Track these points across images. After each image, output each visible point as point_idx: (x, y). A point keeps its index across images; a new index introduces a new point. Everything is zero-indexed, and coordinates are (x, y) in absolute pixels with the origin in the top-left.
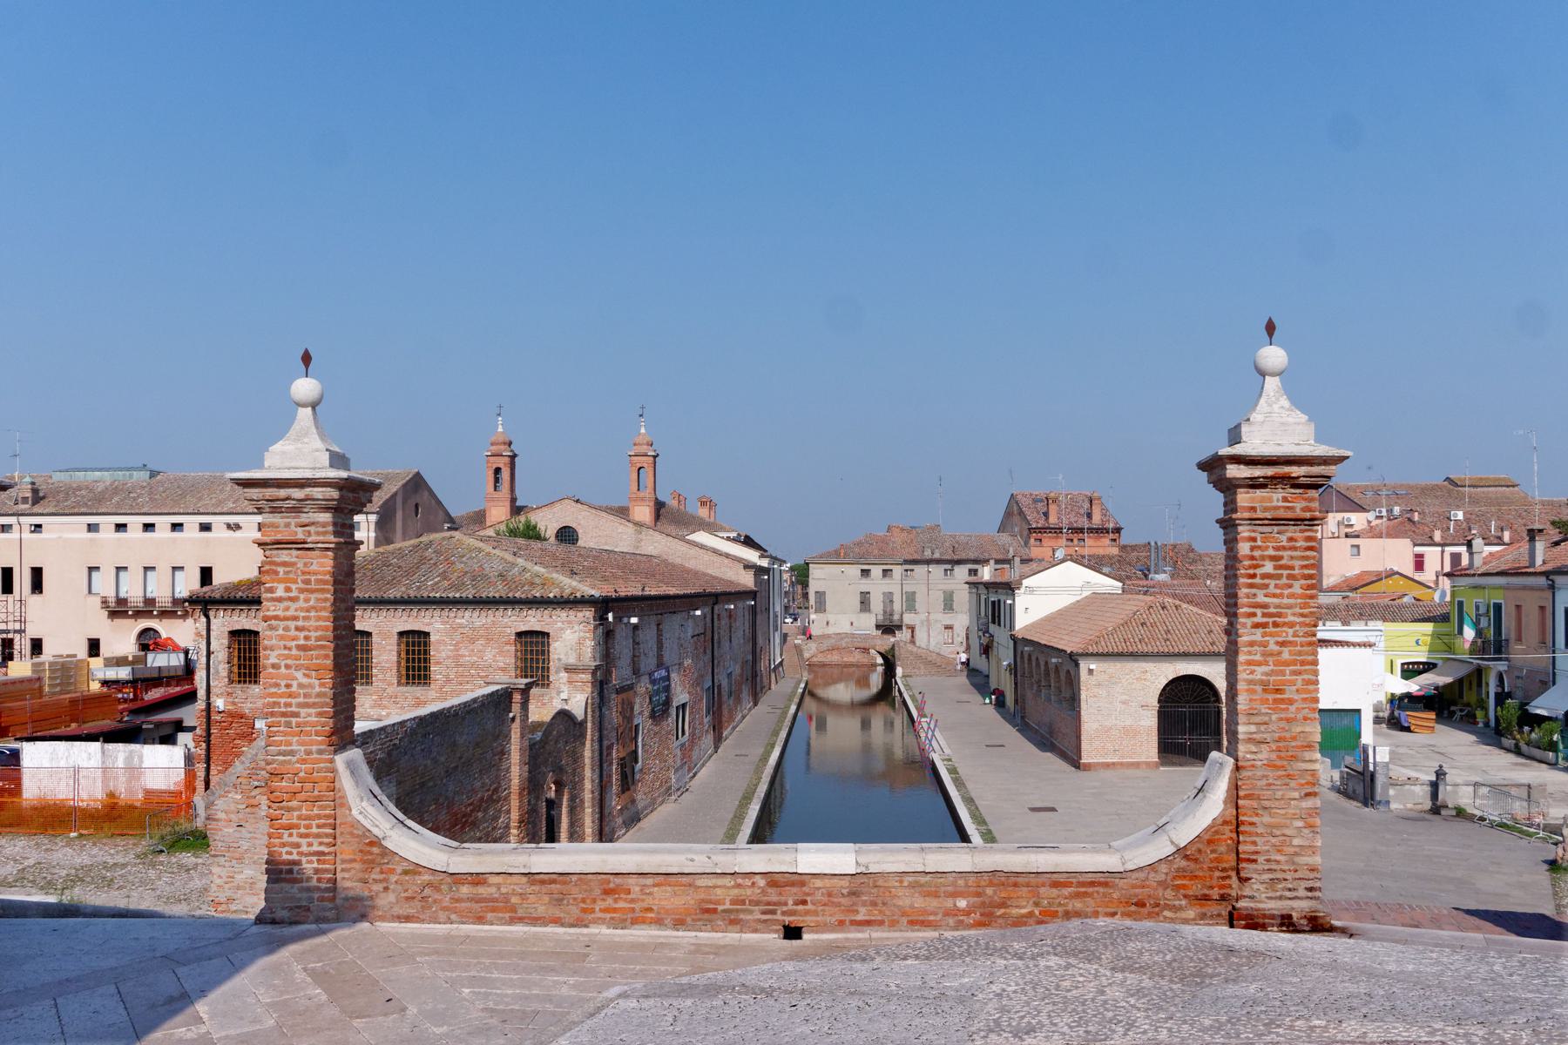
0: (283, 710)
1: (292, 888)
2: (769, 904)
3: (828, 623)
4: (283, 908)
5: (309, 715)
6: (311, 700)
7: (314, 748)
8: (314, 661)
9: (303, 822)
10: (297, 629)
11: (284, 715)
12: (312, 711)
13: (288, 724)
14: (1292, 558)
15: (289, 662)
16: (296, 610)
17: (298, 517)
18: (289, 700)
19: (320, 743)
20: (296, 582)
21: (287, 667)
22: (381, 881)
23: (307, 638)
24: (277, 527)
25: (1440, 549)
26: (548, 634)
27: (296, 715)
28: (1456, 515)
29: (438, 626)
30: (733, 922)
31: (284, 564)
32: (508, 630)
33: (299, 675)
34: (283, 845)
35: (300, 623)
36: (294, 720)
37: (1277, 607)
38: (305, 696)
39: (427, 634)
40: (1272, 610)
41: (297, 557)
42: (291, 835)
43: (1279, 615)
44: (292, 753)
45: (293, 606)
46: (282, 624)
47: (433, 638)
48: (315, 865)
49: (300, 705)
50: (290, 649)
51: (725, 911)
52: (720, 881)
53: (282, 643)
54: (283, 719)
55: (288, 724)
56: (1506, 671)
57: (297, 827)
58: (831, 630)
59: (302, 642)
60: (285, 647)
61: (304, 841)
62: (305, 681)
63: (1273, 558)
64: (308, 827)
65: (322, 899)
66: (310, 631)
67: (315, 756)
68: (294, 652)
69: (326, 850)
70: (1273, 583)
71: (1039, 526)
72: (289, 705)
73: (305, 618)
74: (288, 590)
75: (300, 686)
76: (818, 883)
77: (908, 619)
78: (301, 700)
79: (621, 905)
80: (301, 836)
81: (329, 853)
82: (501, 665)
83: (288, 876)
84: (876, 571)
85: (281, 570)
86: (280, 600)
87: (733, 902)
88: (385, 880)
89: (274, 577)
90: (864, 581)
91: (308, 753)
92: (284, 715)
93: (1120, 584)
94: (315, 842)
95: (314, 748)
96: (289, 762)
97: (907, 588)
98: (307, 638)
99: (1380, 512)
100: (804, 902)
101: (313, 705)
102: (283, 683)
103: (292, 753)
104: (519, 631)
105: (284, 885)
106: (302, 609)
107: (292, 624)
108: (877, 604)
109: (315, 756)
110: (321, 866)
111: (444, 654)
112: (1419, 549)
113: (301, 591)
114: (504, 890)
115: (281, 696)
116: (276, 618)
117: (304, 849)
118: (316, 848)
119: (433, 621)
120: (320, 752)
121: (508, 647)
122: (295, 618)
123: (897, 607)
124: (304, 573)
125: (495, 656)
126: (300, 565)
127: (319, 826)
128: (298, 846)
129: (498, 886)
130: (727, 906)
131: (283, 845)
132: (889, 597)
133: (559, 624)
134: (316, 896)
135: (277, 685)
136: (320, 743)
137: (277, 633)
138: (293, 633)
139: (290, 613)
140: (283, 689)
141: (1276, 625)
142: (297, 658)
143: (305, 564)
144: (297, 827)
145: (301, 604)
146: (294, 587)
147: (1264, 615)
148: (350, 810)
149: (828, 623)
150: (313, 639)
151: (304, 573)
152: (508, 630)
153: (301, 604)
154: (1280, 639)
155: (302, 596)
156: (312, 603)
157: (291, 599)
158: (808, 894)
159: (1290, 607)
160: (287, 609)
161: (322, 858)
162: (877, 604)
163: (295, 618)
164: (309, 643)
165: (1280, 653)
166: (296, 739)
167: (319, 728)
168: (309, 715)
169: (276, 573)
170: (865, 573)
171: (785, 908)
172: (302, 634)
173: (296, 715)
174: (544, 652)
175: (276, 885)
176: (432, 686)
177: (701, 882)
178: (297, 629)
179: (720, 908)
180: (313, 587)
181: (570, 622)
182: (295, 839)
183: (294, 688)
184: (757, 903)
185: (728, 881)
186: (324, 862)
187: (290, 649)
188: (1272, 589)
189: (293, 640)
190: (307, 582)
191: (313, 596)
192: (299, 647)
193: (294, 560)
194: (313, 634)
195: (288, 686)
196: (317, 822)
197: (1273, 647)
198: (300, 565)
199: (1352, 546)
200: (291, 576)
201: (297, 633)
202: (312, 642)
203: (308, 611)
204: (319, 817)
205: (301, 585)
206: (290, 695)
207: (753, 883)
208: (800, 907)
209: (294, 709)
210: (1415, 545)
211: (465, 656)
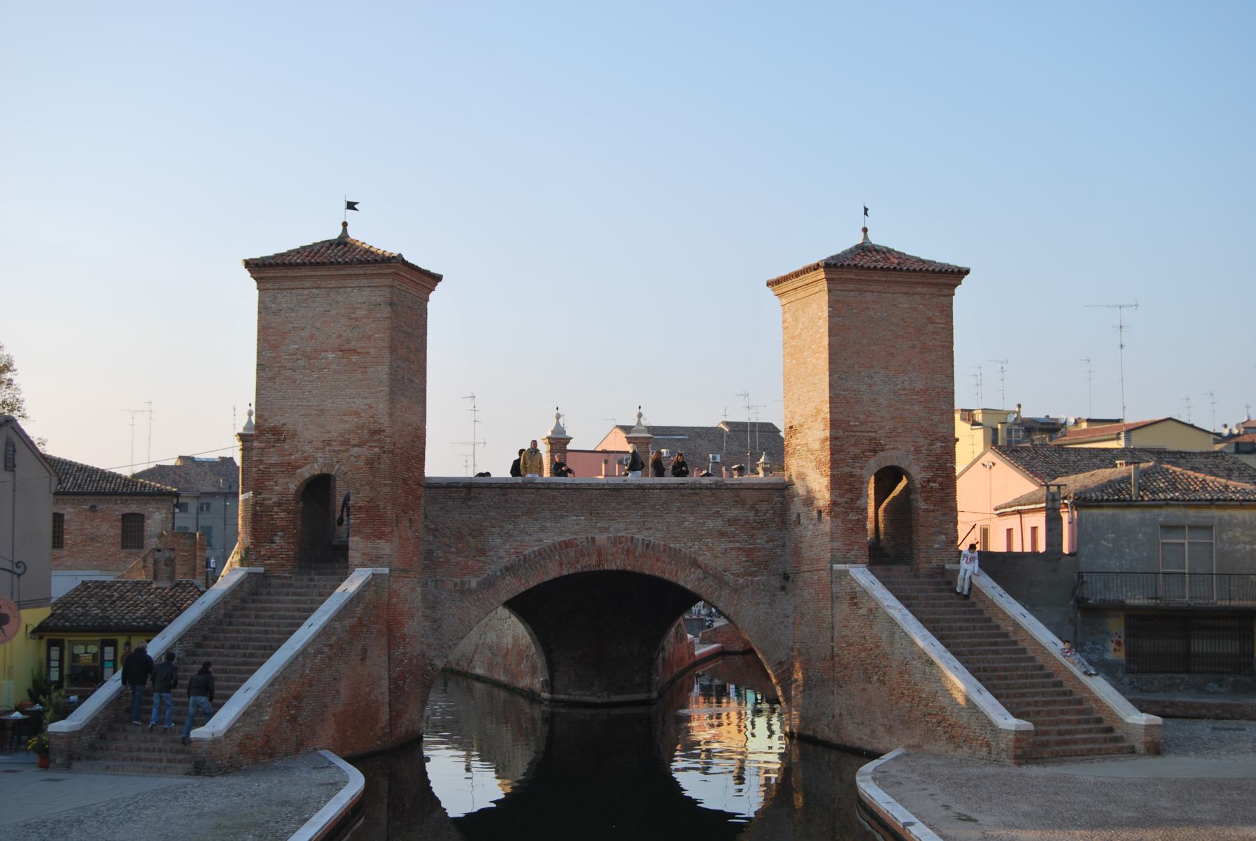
26: (143, 515)
28: (714, 458)
29: (71, 510)
32: (117, 513)
39: (62, 515)
47: (66, 518)
82: (112, 534)
97: (202, 523)
104: (124, 513)
111: (73, 528)
119: (66, 507)
121: (117, 523)
125: (108, 529)
133: (151, 509)
152: (117, 513)
174: (141, 529)
176: (65, 548)
181: (158, 508)
211: (88, 529)
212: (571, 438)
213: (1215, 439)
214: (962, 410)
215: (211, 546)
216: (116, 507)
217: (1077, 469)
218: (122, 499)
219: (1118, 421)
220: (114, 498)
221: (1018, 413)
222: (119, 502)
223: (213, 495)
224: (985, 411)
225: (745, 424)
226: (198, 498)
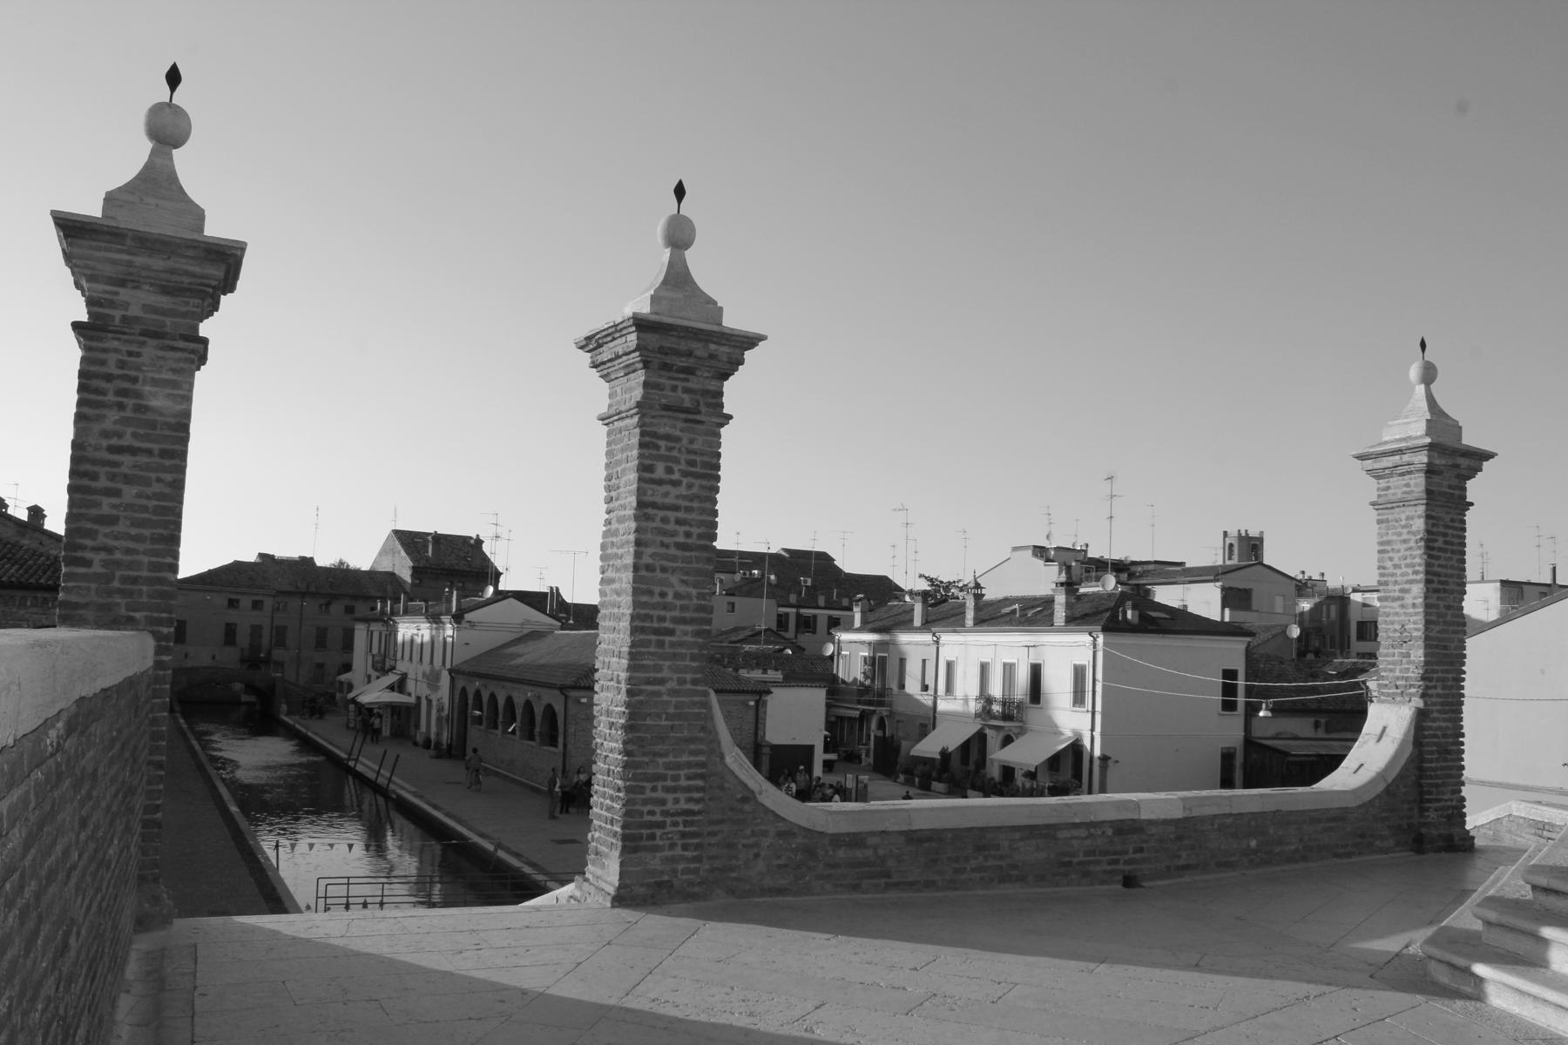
0: (656, 625)
1: (654, 857)
2: (1115, 853)
3: (186, 655)
4: (642, 885)
5: (686, 634)
6: (688, 615)
7: (689, 676)
8: (694, 565)
9: (670, 773)
10: (679, 522)
11: (657, 632)
12: (689, 628)
13: (661, 644)
14: (1453, 536)
15: (665, 563)
16: (677, 497)
17: (687, 380)
18: (662, 613)
19: (695, 670)
20: (677, 461)
21: (664, 570)
22: (752, 846)
23: (688, 535)
24: (662, 390)
25: (794, 610)
27: (671, 632)
28: (805, 582)
30: (1086, 874)
31: (668, 437)
33: (674, 579)
34: (645, 802)
35: (681, 515)
36: (667, 639)
37: (1446, 575)
38: (683, 608)
40: (1443, 579)
41: (682, 430)
42: (654, 789)
43: (1446, 583)
44: (662, 681)
45: (674, 491)
46: (661, 514)
48: (681, 828)
49: (676, 621)
50: (667, 547)
51: (1080, 863)
52: (1075, 833)
53: (659, 539)
54: (654, 638)
55: (661, 644)
56: (887, 716)
57: (663, 778)
58: (189, 663)
59: (681, 539)
60: (663, 544)
61: (670, 797)
62: (682, 589)
63: (1445, 535)
64: (676, 778)
65: (687, 871)
66: (691, 526)
67: (689, 686)
68: (673, 551)
69: (696, 808)
70: (1443, 555)
71: (421, 565)
72: (662, 619)
73: (689, 510)
74: (669, 471)
75: (677, 596)
76: (1153, 830)
77: (278, 654)
78: (676, 613)
79: (991, 862)
80: (668, 790)
81: (699, 813)
83: (650, 843)
84: (245, 602)
85: (662, 443)
86: (660, 482)
87: (1087, 853)
88: (756, 845)
89: (654, 452)
90: (231, 611)
91: (681, 682)
92: (657, 632)
93: (560, 624)
94: (682, 796)
95: (689, 676)
96: (658, 694)
98: (688, 535)
99: (745, 574)
100: (1141, 850)
101: (691, 621)
102: (657, 590)
103: (662, 681)
105: (642, 854)
106: (684, 497)
107: (672, 515)
108: (243, 639)
109: (689, 686)
110: (687, 829)
112: (783, 610)
113: (685, 474)
114: (881, 852)
115: (654, 606)
116: (654, 505)
117: (670, 806)
118: (683, 806)
120: (695, 682)
122: (676, 508)
123: (265, 641)
124: (689, 452)
126: (685, 442)
127: (689, 778)
128: (663, 802)
129: (876, 848)
130: (1081, 858)
131: (645, 802)
132: (256, 631)
134: (680, 867)
135: (651, 593)
136: (695, 670)
137: (655, 525)
138: (671, 527)
139: (669, 500)
140: (656, 599)
141: (1445, 591)
142: (674, 559)
143: (692, 441)
144: (663, 778)
145: (682, 490)
146: (676, 468)
147: (1439, 582)
148: (722, 757)
149: (186, 655)
150: (694, 536)
151: (689, 452)
153: (682, 490)
154: (1446, 603)
155: (685, 481)
156: (695, 490)
157: (676, 484)
158: (1146, 842)
159: (1451, 576)
160: (666, 494)
161: (689, 818)
162: (243, 639)
163: (676, 508)
164: (689, 541)
165: (1447, 614)
166: (668, 663)
167: (696, 651)
168: (686, 634)
169: (657, 447)
170: (233, 604)
171: (1126, 857)
172: (682, 529)
173: (671, 632)
175: (633, 856)
177: (1062, 834)
178: (679, 522)
179: (1075, 860)
180: (698, 470)
182: (659, 794)
183: (670, 598)
184: (1106, 853)
185: (1082, 833)
186: (692, 823)
187: (667, 547)
188: (1442, 562)
189: (672, 536)
190: (692, 463)
191: (697, 482)
192: (679, 546)
193: (678, 433)
194: (695, 531)
195: (663, 595)
196: (686, 771)
197: (1443, 610)
198: (685, 442)
199: (729, 603)
200: (675, 453)
201: (678, 528)
202: (692, 541)
203: (691, 500)
204: (689, 765)
205: (683, 466)
206: (665, 607)
207: (1103, 833)
208: (1138, 856)
209: (667, 625)
210: (779, 606)
212: (1488, 456)
213: (1297, 586)
214: (1035, 547)
215: (284, 646)
216: (22, 612)
217: (1155, 610)
218: (36, 598)
219: (1181, 563)
220: (19, 594)
221: (1086, 551)
222: (29, 603)
223: (289, 594)
224: (1058, 549)
225: (811, 552)
226: (274, 596)
